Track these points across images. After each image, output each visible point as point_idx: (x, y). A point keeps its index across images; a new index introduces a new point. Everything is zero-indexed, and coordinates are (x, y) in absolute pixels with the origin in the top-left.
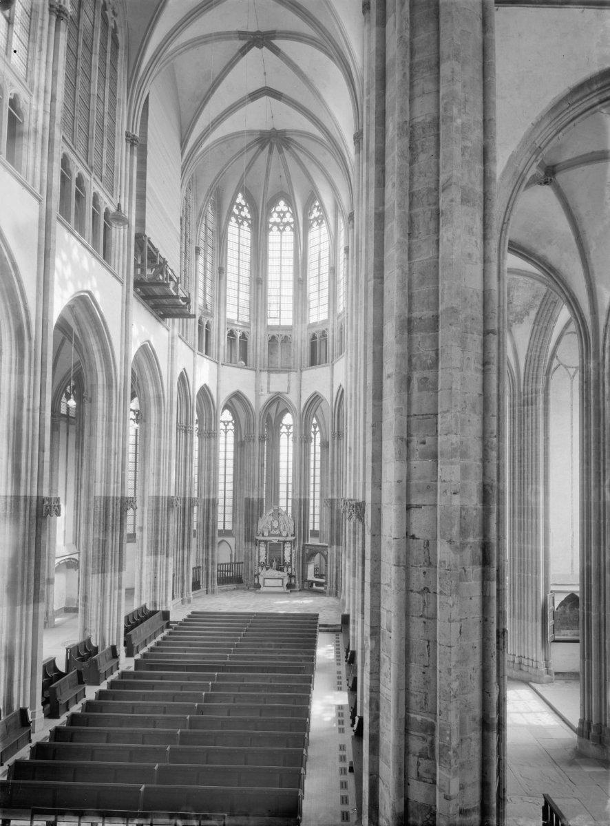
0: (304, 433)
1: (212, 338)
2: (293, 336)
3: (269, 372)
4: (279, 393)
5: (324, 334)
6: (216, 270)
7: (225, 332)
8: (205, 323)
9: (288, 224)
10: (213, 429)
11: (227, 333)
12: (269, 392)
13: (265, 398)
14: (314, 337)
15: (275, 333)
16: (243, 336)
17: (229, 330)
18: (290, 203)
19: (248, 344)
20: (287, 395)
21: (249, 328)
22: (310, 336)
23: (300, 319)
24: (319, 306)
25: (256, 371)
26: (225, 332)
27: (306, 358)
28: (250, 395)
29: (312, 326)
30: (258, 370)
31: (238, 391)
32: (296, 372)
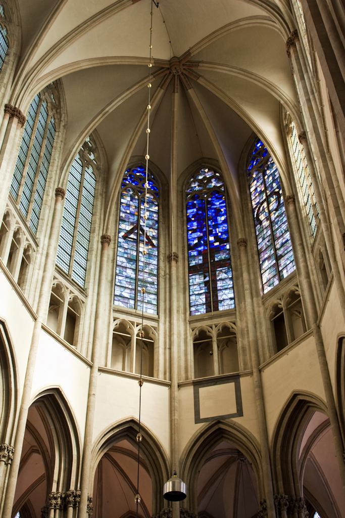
0: (281, 490)
1: (81, 326)
2: (239, 323)
3: (197, 384)
4: (218, 421)
5: (294, 296)
6: (97, 239)
7: (109, 326)
8: (68, 298)
9: (215, 192)
10: (72, 488)
11: (113, 326)
12: (198, 420)
13: (190, 430)
14: (277, 309)
15: (204, 324)
16: (146, 331)
17: (118, 322)
18: (215, 168)
19: (155, 346)
20: (237, 420)
21: (157, 321)
22: (269, 312)
23: (247, 293)
24: (278, 258)
25: (169, 386)
26: (109, 326)
27: (266, 344)
28: (156, 425)
29: (265, 298)
30: (175, 383)
31: (132, 421)
32: (251, 374)
